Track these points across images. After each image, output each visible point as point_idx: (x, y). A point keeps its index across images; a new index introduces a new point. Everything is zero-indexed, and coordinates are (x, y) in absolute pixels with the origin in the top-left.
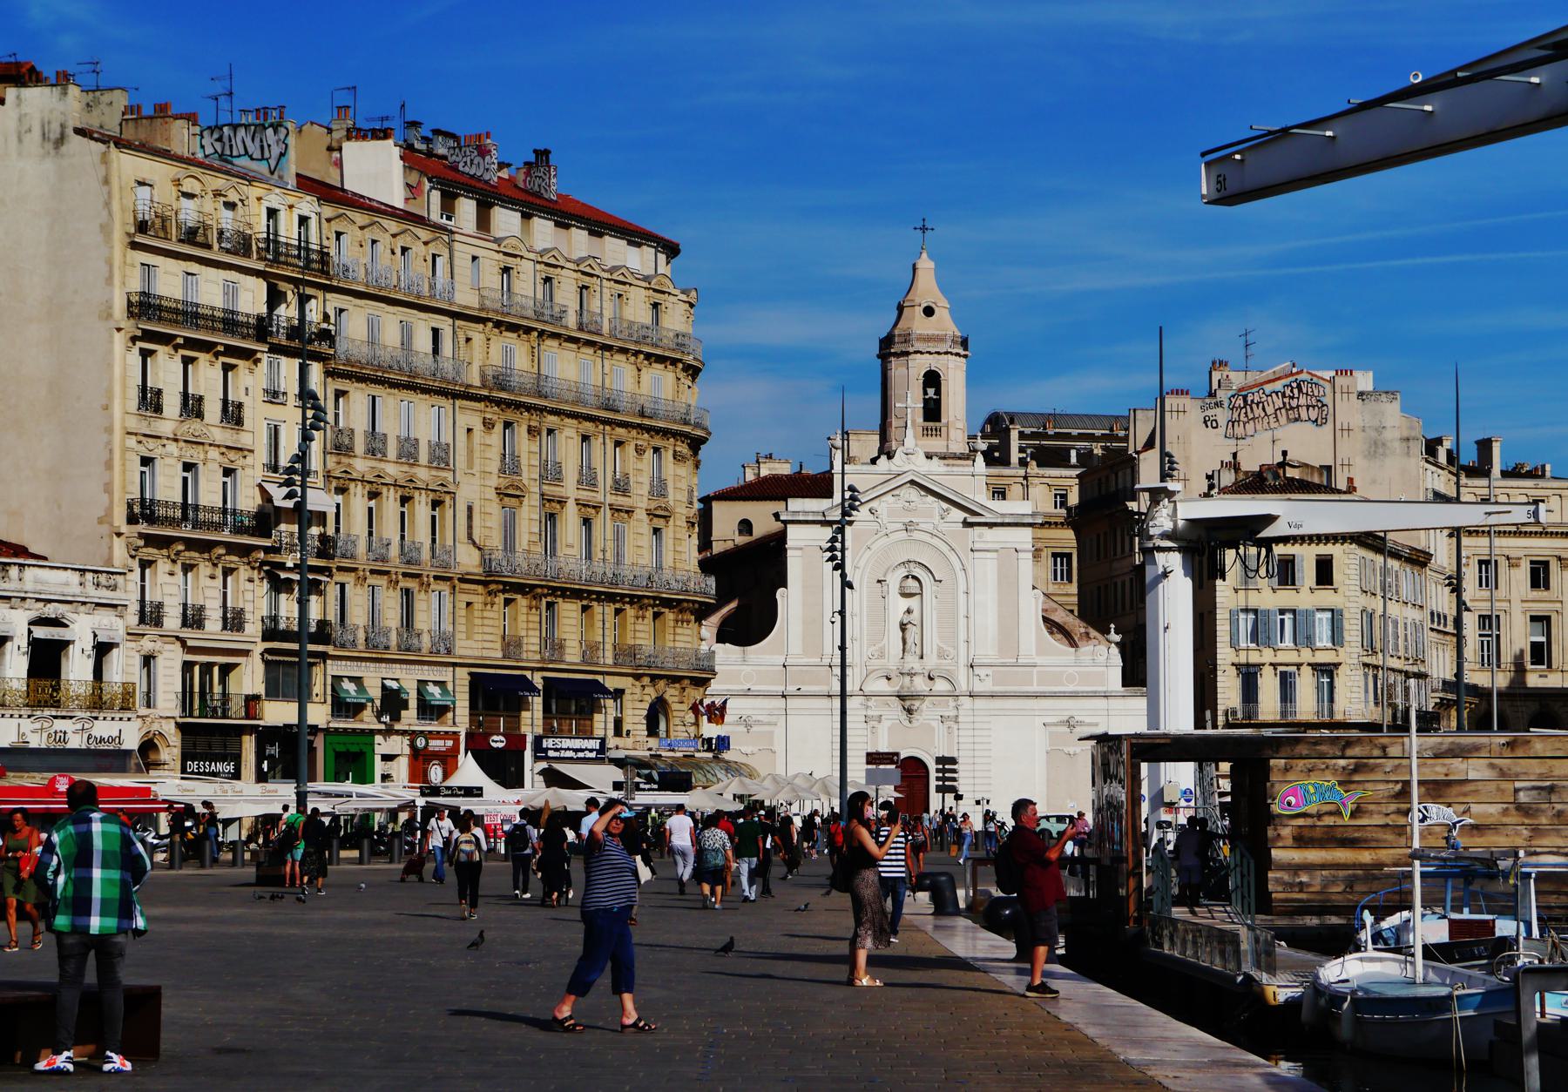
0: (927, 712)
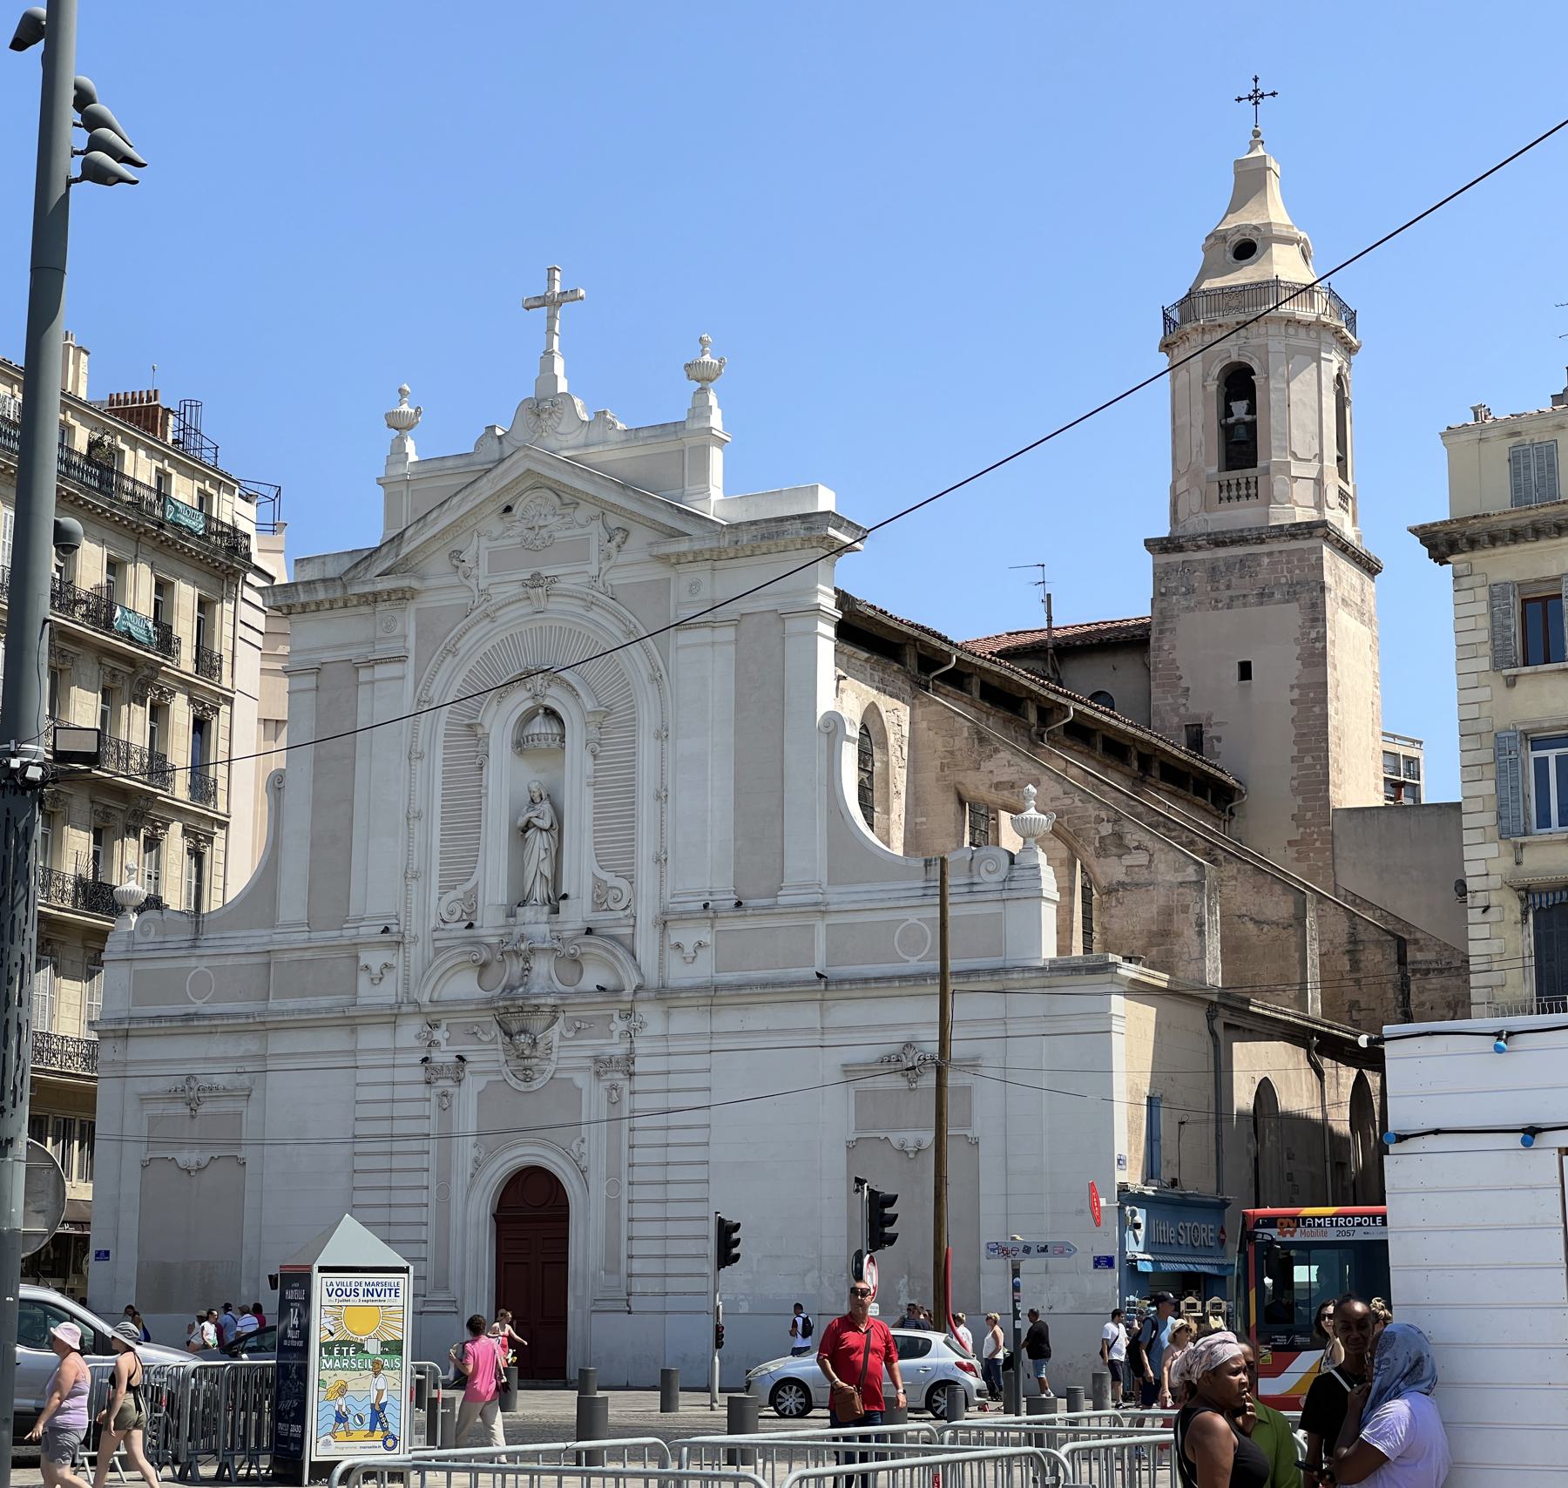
0: (566, 1052)
